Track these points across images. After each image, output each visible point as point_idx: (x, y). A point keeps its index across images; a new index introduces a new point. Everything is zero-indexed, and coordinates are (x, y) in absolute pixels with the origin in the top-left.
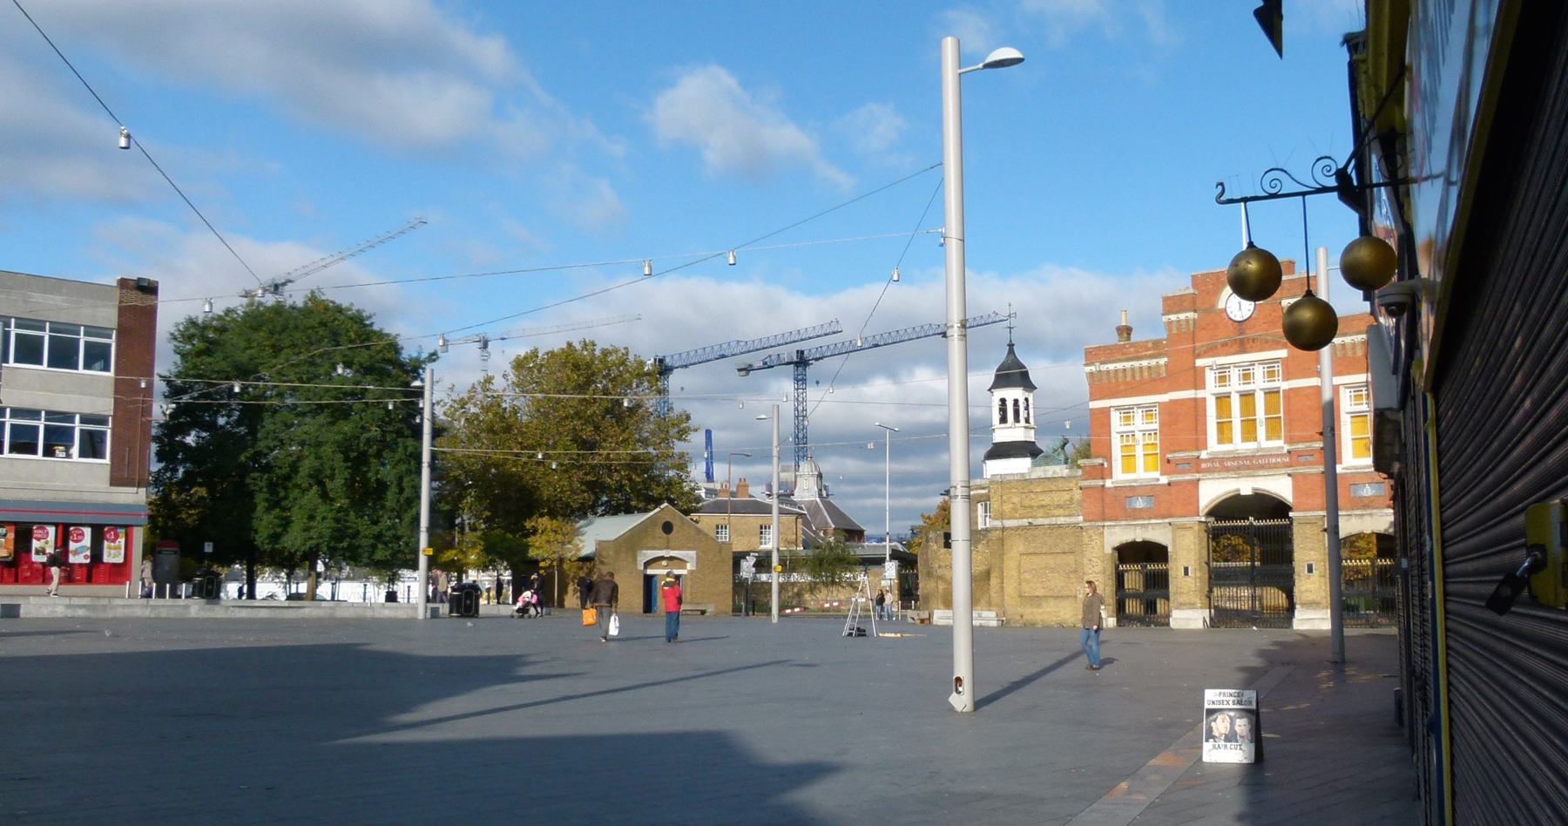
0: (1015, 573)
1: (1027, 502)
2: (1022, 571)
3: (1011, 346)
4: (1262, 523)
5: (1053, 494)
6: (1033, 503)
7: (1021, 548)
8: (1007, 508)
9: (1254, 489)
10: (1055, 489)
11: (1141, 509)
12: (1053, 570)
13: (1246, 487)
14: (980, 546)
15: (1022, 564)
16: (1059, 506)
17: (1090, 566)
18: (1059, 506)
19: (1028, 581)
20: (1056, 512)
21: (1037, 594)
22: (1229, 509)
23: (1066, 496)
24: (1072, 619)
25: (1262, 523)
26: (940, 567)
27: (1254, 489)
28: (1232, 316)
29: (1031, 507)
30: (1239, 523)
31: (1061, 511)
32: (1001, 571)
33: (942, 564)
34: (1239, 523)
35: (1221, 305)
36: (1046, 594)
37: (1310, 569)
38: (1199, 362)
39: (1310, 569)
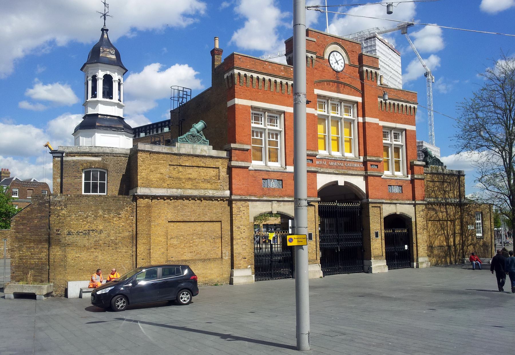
0: (162, 239)
1: (175, 174)
2: (169, 237)
4: (341, 205)
5: (201, 170)
6: (180, 175)
7: (170, 217)
8: (154, 177)
9: (345, 182)
10: (203, 165)
11: (274, 189)
12: (200, 236)
13: (341, 180)
14: (123, 213)
15: (169, 231)
16: (205, 181)
17: (239, 233)
18: (205, 181)
19: (174, 246)
20: (202, 185)
21: (185, 258)
23: (212, 172)
24: (219, 279)
25: (341, 205)
26: (69, 234)
27: (345, 182)
28: (333, 66)
29: (179, 179)
30: (330, 204)
31: (209, 185)
32: (149, 236)
33: (72, 230)
34: (330, 204)
35: (326, 57)
36: (195, 258)
37: (377, 235)
39: (377, 235)
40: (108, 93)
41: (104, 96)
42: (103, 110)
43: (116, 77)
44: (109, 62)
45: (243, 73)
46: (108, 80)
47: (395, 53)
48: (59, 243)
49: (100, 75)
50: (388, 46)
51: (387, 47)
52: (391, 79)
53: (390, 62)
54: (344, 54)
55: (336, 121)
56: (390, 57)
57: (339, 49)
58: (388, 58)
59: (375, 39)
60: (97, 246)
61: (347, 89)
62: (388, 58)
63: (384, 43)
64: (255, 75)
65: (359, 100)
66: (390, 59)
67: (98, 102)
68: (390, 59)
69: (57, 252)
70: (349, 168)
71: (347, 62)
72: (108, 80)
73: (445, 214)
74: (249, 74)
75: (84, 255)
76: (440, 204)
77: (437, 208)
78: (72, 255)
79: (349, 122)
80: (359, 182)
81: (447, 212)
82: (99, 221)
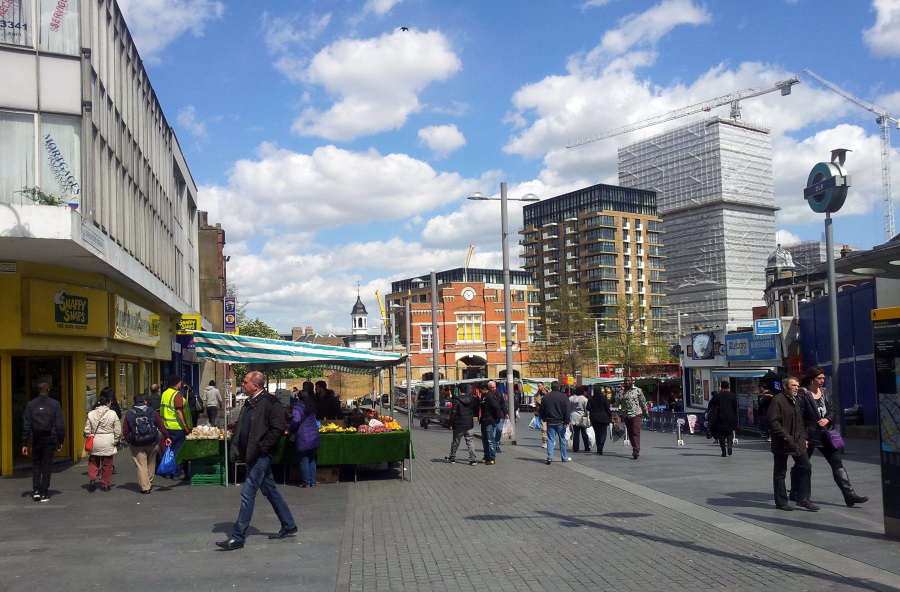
3: (359, 297)
22: (465, 360)
35: (462, 294)
38: (455, 313)
40: (361, 325)
41: (359, 326)
42: (359, 333)
43: (363, 318)
44: (361, 313)
45: (415, 311)
46: (360, 320)
47: (759, 133)
48: (344, 386)
49: (357, 318)
50: (744, 128)
51: (741, 128)
52: (749, 169)
53: (747, 147)
54: (473, 290)
55: (469, 325)
56: (748, 141)
57: (470, 289)
58: (743, 143)
59: (718, 125)
60: (357, 387)
61: (475, 308)
62: (743, 143)
63: (735, 126)
64: (422, 311)
65: (483, 312)
66: (747, 144)
67: (356, 330)
68: (747, 144)
69: (343, 389)
70: (476, 349)
71: (475, 294)
72: (360, 320)
73: (546, 369)
74: (419, 311)
75: (352, 390)
76: (542, 363)
77: (540, 365)
78: (348, 390)
79: (477, 325)
80: (483, 355)
81: (548, 368)
82: (357, 378)
